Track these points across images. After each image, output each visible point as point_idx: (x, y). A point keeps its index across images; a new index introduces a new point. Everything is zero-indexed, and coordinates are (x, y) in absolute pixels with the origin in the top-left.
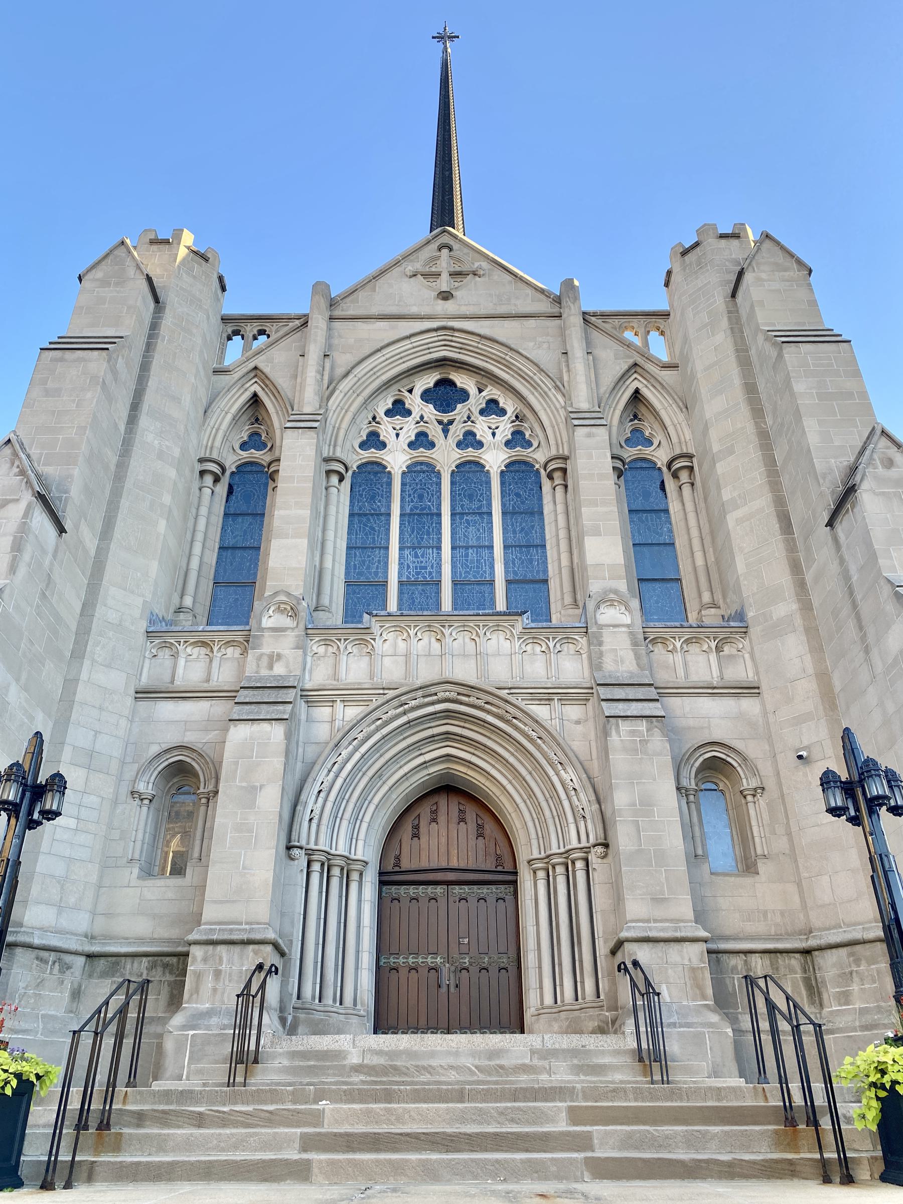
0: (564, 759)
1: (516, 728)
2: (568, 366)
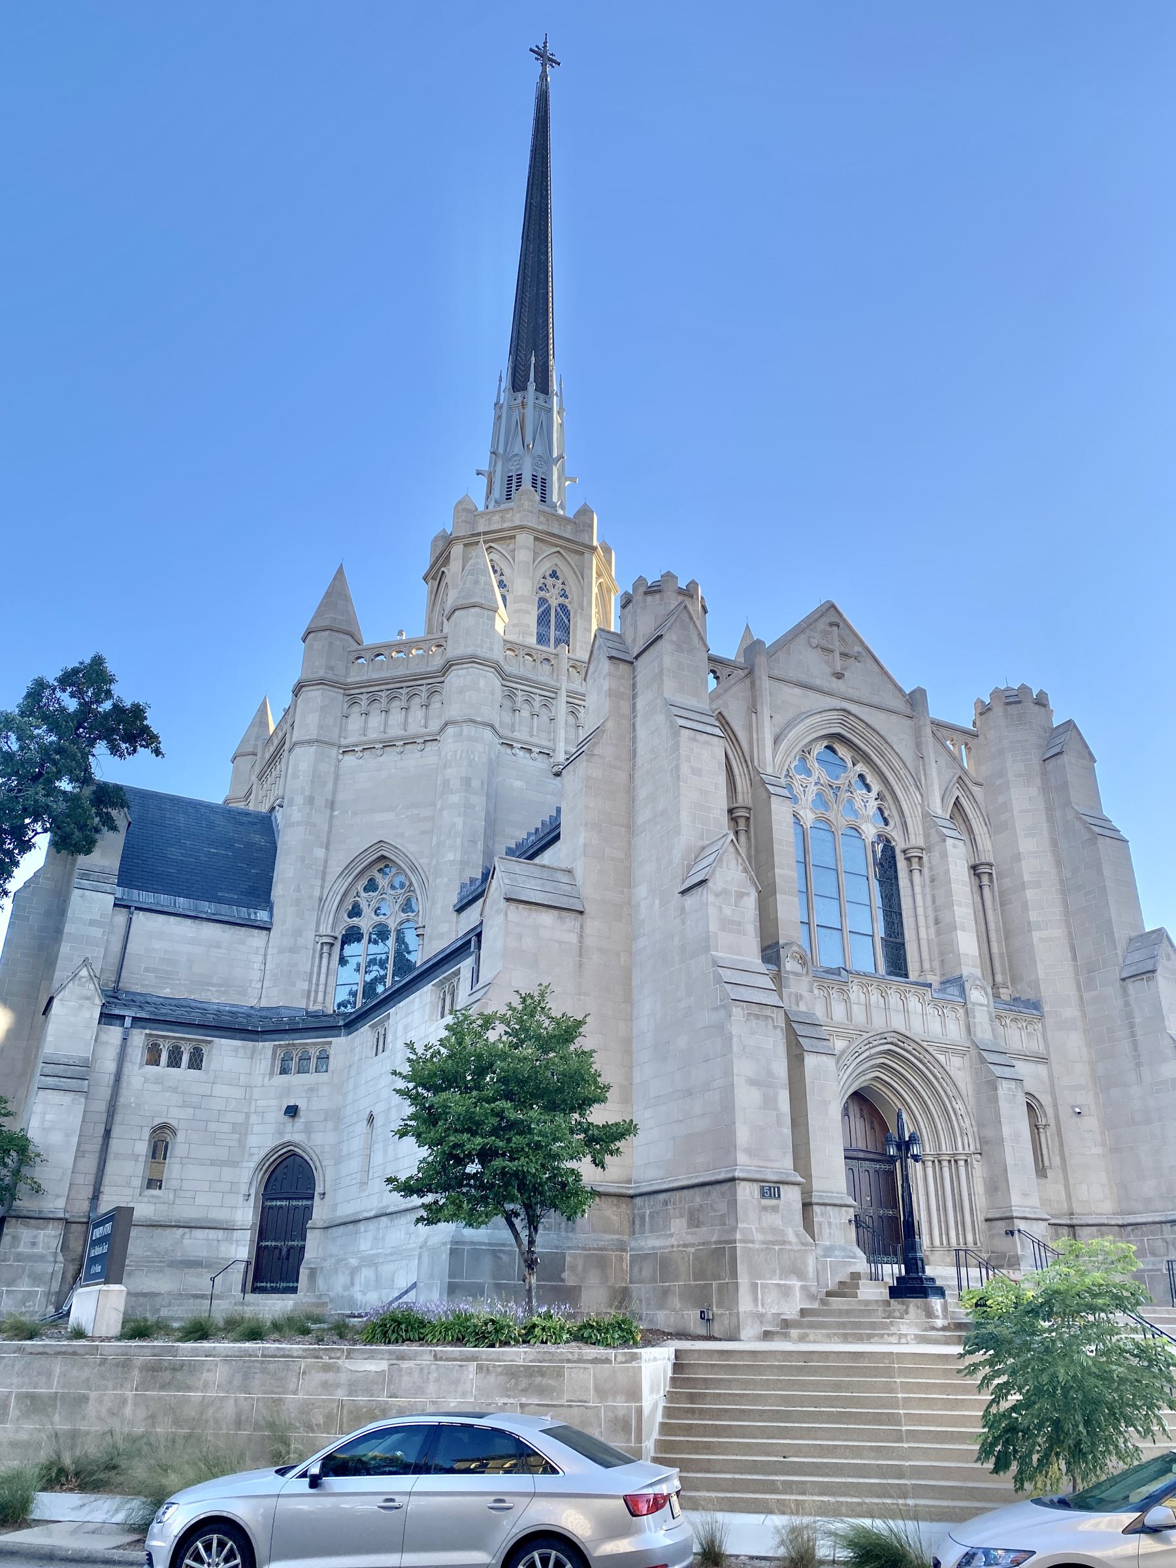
0: (957, 1095)
1: (927, 1068)
2: (924, 770)
